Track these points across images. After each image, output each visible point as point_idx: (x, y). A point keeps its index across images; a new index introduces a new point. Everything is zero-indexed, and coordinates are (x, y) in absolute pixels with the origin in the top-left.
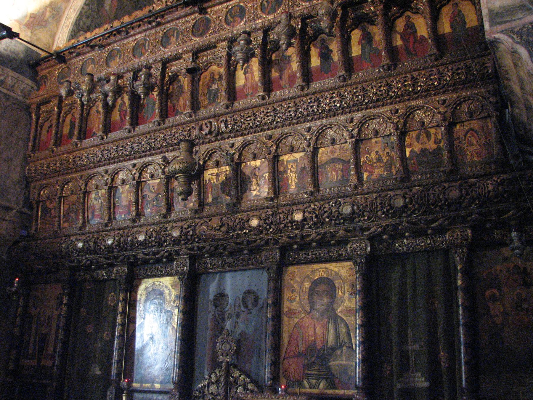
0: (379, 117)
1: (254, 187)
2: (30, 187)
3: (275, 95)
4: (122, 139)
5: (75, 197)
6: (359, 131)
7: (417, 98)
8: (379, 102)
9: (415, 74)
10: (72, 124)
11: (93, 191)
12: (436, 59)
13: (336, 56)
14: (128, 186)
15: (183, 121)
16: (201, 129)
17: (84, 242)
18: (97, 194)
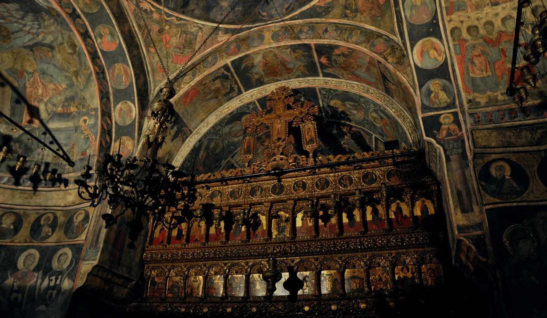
0: (381, 256)
1: (305, 287)
2: (144, 267)
3: (322, 236)
5: (178, 279)
6: (370, 263)
7: (403, 249)
8: (382, 248)
9: (403, 236)
10: (180, 231)
12: (414, 230)
13: (358, 219)
14: (219, 276)
17: (186, 308)
18: (195, 278)
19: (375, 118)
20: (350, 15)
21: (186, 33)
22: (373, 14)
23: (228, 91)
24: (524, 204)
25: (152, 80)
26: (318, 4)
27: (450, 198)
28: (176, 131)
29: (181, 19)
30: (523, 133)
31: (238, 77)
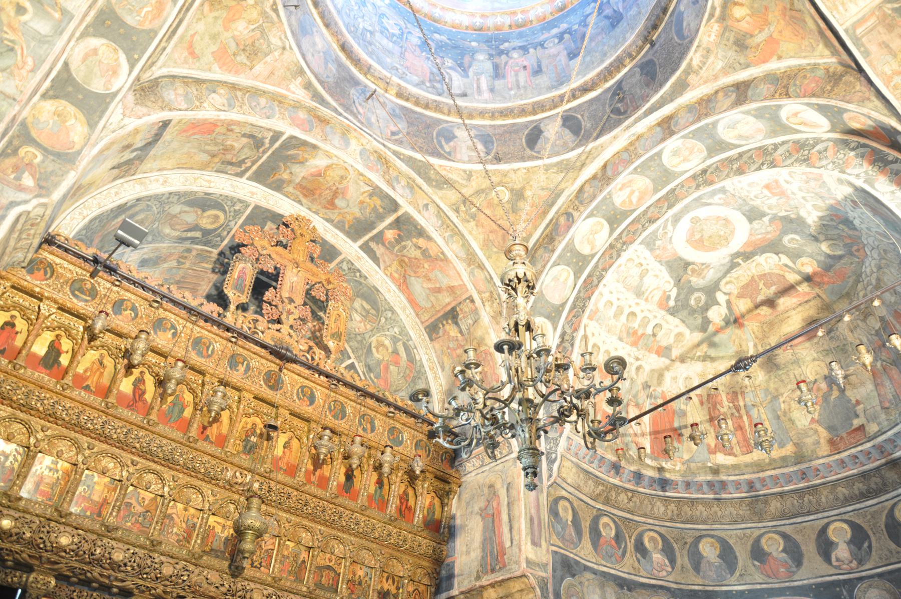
4: (135, 425)
11: (51, 455)
15: (218, 455)
16: (235, 476)
19: (380, 345)
20: (462, 214)
21: (263, 32)
22: (491, 238)
23: (234, 160)
24: (577, 558)
25: (168, 50)
26: (437, 168)
27: (523, 521)
28: (130, 160)
29: (276, 11)
30: (590, 482)
31: (268, 157)
